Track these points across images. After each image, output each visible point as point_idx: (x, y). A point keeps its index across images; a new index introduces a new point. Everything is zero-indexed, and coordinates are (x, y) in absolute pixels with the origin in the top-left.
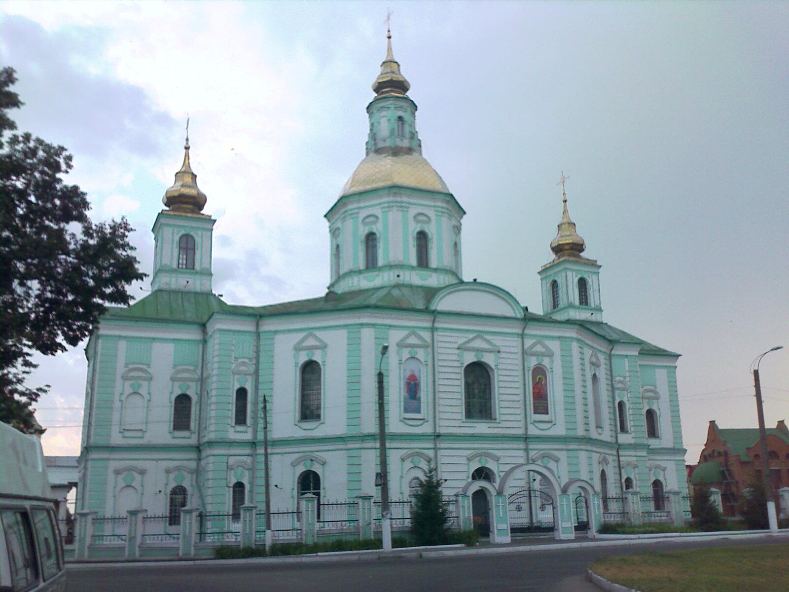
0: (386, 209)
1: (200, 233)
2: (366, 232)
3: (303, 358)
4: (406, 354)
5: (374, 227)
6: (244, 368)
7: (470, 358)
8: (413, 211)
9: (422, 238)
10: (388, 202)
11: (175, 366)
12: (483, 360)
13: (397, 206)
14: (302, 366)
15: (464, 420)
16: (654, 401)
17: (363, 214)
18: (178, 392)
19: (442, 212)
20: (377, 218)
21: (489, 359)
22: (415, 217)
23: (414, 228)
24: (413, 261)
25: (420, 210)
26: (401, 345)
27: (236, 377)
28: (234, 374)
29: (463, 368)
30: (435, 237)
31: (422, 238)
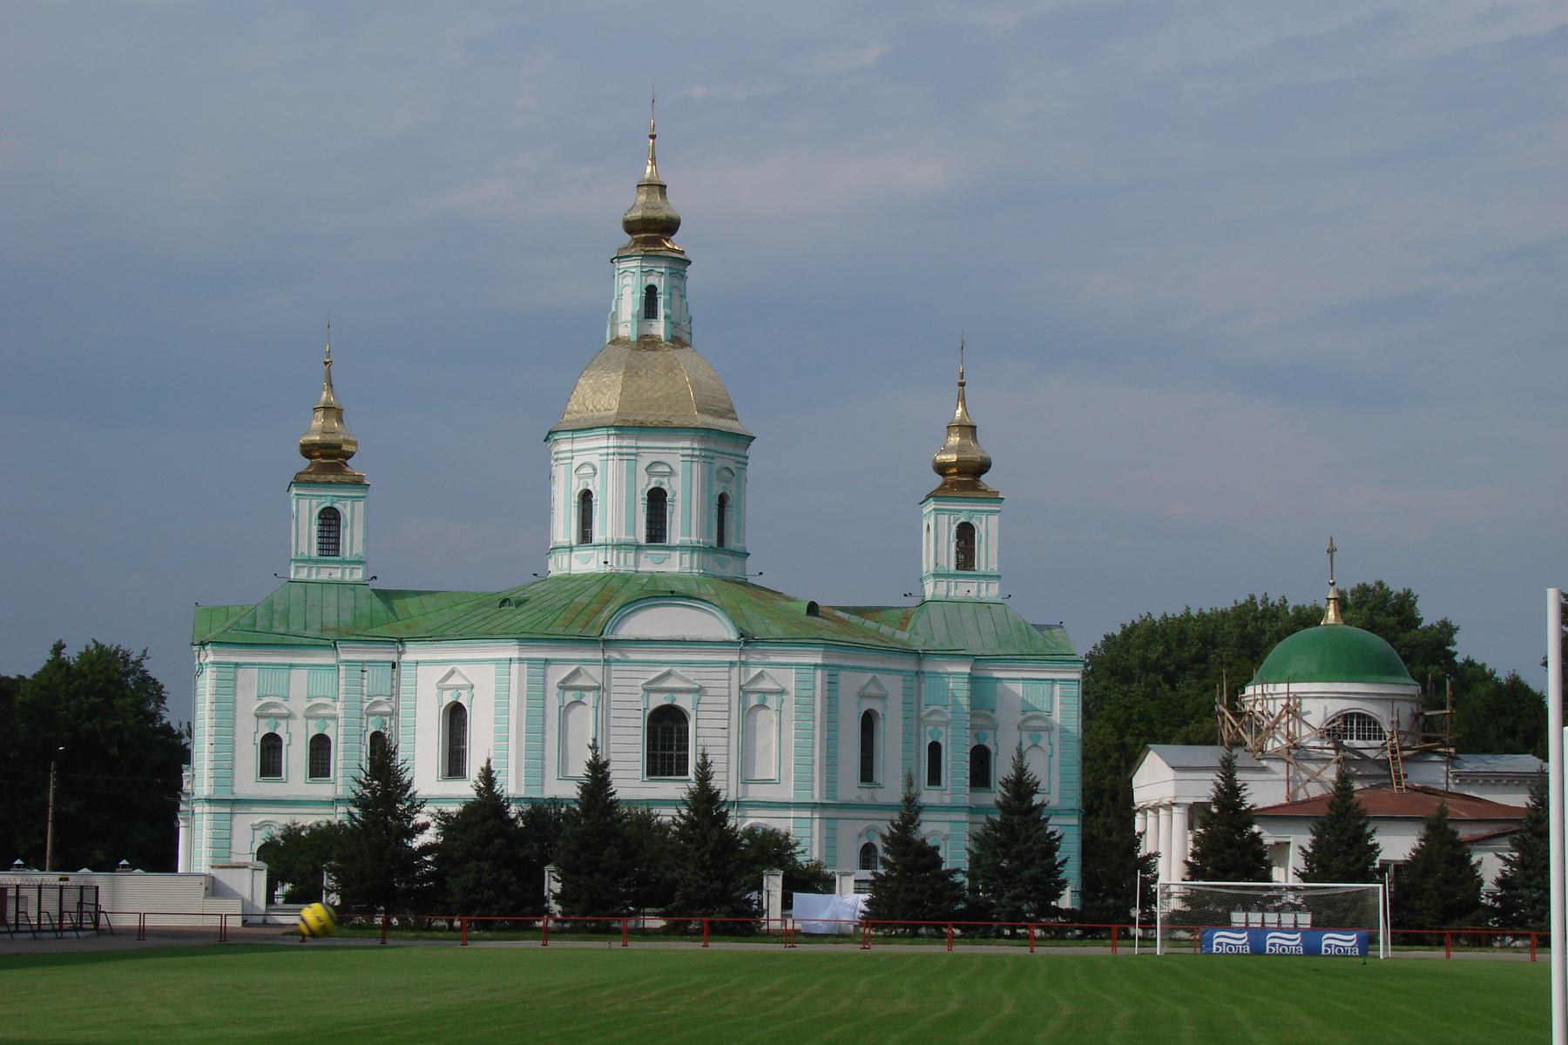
0: (605, 457)
2: (581, 488)
3: (448, 698)
4: (570, 697)
5: (590, 481)
8: (644, 462)
9: (657, 500)
10: (608, 447)
11: (310, 698)
12: (676, 703)
13: (620, 454)
14: (449, 704)
15: (645, 779)
16: (1042, 733)
17: (576, 463)
18: (314, 732)
19: (692, 456)
20: (595, 469)
21: (685, 702)
23: (645, 484)
24: (642, 538)
25: (654, 458)
26: (564, 686)
27: (371, 719)
28: (369, 715)
29: (648, 712)
30: (679, 498)
31: (657, 500)
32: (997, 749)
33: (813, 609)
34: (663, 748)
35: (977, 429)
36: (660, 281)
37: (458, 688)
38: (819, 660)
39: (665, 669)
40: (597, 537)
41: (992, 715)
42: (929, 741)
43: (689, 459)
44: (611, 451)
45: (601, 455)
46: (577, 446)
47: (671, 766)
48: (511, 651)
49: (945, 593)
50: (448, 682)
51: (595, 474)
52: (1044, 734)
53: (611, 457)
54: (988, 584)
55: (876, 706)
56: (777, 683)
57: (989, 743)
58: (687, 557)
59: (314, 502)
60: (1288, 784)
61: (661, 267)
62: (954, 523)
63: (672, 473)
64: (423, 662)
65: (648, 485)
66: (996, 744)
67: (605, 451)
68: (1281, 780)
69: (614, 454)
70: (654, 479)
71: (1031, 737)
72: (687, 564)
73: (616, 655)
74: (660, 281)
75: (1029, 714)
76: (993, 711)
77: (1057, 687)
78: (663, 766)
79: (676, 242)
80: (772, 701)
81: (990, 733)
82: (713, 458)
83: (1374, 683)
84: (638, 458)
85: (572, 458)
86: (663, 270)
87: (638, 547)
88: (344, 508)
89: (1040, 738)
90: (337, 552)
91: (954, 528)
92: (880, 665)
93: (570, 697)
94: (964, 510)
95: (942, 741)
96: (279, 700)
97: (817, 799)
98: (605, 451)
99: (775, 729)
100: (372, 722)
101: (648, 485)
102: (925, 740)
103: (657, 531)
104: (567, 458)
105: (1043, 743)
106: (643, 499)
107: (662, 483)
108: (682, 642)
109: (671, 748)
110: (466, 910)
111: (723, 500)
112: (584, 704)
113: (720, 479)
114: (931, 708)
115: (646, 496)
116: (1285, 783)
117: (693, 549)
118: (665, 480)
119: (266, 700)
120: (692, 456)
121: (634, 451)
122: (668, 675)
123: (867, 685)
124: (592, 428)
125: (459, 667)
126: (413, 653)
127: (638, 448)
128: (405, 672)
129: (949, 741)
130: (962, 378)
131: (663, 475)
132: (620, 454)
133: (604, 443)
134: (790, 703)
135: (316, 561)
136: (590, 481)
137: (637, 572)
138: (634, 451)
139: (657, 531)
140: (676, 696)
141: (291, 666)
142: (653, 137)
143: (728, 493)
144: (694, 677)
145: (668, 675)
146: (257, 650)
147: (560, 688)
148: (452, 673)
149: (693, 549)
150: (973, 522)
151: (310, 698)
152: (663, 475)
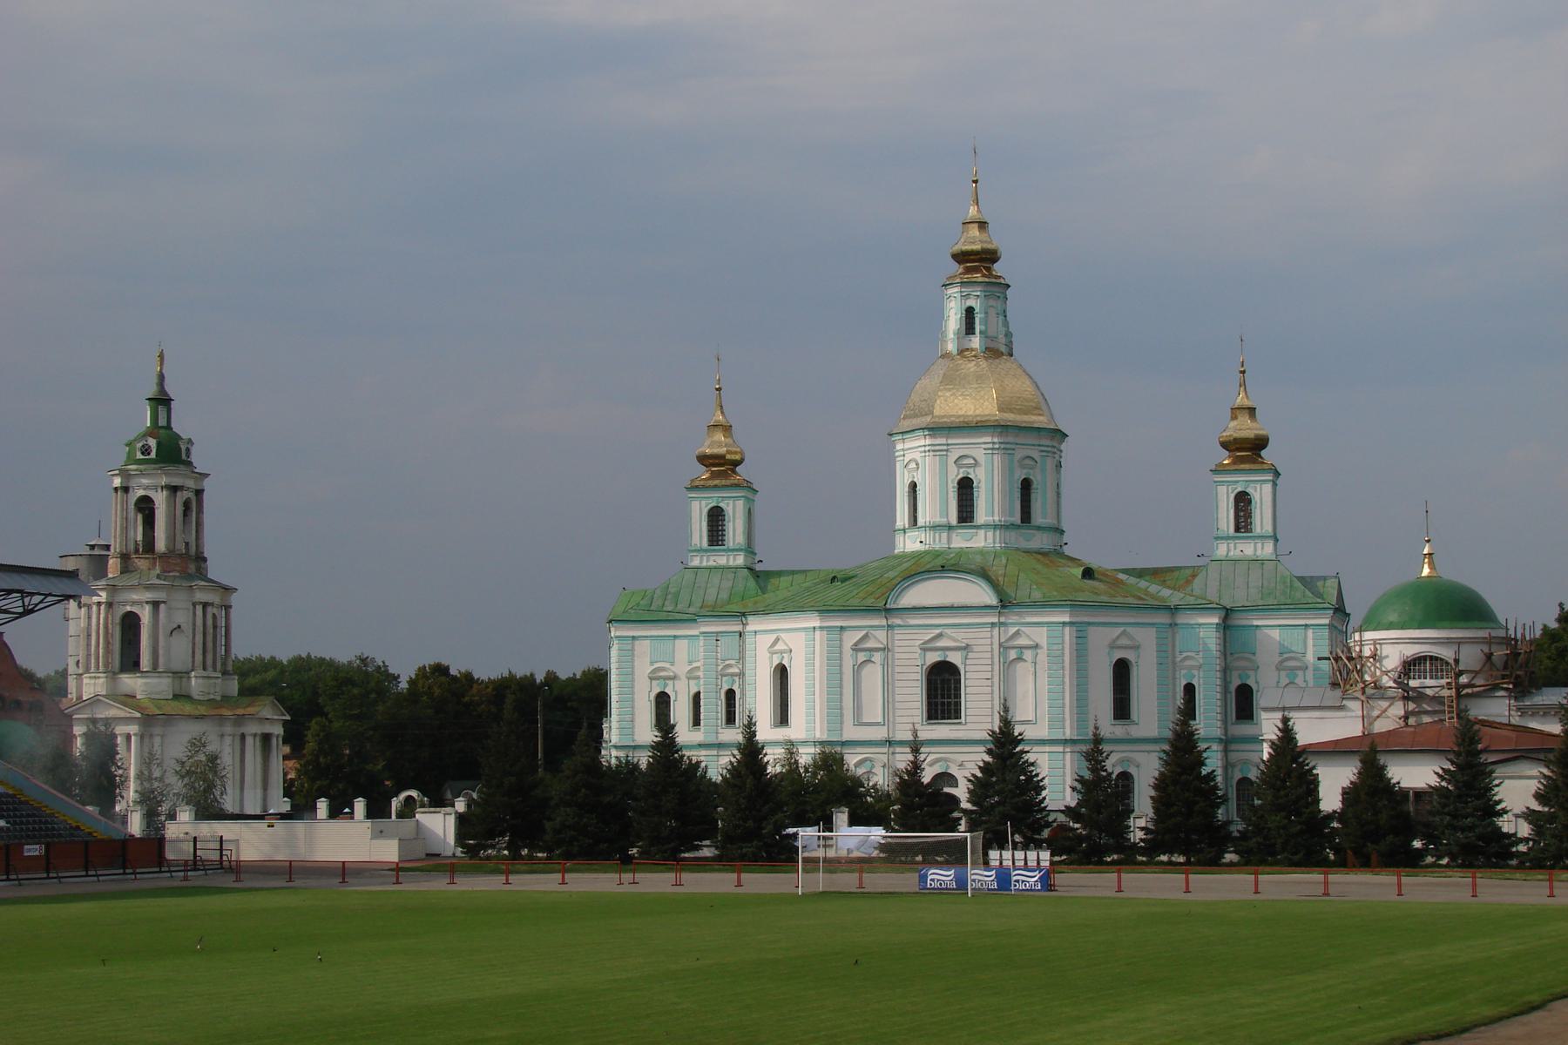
0: (923, 454)
1: (731, 502)
4: (862, 657)
6: (731, 670)
7: (933, 658)
8: (954, 456)
9: (965, 486)
10: (925, 446)
12: (948, 659)
13: (934, 451)
15: (925, 723)
19: (993, 449)
21: (955, 658)
22: (955, 462)
23: (955, 475)
24: (954, 520)
26: (856, 648)
27: (724, 679)
28: (723, 676)
29: (925, 667)
30: (983, 485)
31: (965, 486)
32: (1258, 687)
33: (1088, 573)
34: (943, 697)
35: (1257, 411)
36: (977, 303)
37: (782, 652)
38: (1067, 619)
39: (937, 631)
40: (921, 521)
41: (1253, 658)
42: (1184, 683)
43: (990, 452)
44: (927, 448)
45: (921, 452)
46: (907, 445)
47: (949, 712)
48: (813, 621)
49: (1225, 553)
50: (776, 648)
51: (918, 468)
52: (1300, 673)
53: (927, 454)
54: (1263, 544)
55: (1129, 655)
56: (1031, 639)
57: (1251, 682)
58: (990, 534)
59: (703, 503)
60: (1363, 720)
61: (976, 291)
62: (1232, 492)
63: (976, 464)
64: (759, 631)
65: (957, 476)
66: (1257, 682)
67: (923, 449)
68: (1356, 717)
69: (929, 451)
70: (962, 470)
71: (1287, 676)
72: (990, 540)
73: (898, 621)
74: (977, 303)
75: (1285, 656)
76: (1254, 654)
77: (1310, 632)
78: (943, 711)
79: (998, 268)
80: (1028, 655)
81: (1251, 673)
82: (1014, 449)
83: (1456, 628)
84: (949, 454)
85: (904, 455)
86: (978, 293)
87: (950, 528)
88: (728, 507)
89: (1296, 676)
90: (916, 525)
91: (1232, 496)
92: (1132, 620)
93: (862, 657)
94: (1240, 482)
95: (1195, 682)
96: (667, 665)
97: (1068, 736)
98: (923, 449)
99: (1031, 678)
100: (726, 682)
101: (957, 476)
102: (1180, 682)
103: (966, 513)
104: (901, 456)
105: (1299, 680)
106: (954, 487)
107: (968, 473)
108: (952, 608)
109: (949, 697)
110: (549, 850)
111: (749, 509)
112: (874, 662)
113: (1023, 467)
114: (1185, 654)
115: (956, 485)
116: (1361, 719)
117: (995, 527)
118: (971, 470)
119: (656, 665)
120: (993, 449)
121: (945, 448)
122: (940, 636)
123: (1118, 637)
124: (913, 430)
125: (783, 635)
126: (754, 624)
127: (948, 445)
128: (749, 639)
129: (1201, 681)
130: (1243, 366)
131: (969, 466)
132: (934, 451)
133: (922, 442)
134: (1042, 655)
135: (706, 551)
136: (915, 474)
137: (949, 548)
138: (945, 448)
139: (966, 513)
140: (947, 653)
141: (675, 637)
142: (975, 182)
143: (1031, 477)
144: (961, 637)
145: (940, 636)
146: (649, 625)
147: (853, 650)
148: (777, 640)
149: (995, 527)
150: (1249, 490)
151: (690, 662)
152: (969, 466)
